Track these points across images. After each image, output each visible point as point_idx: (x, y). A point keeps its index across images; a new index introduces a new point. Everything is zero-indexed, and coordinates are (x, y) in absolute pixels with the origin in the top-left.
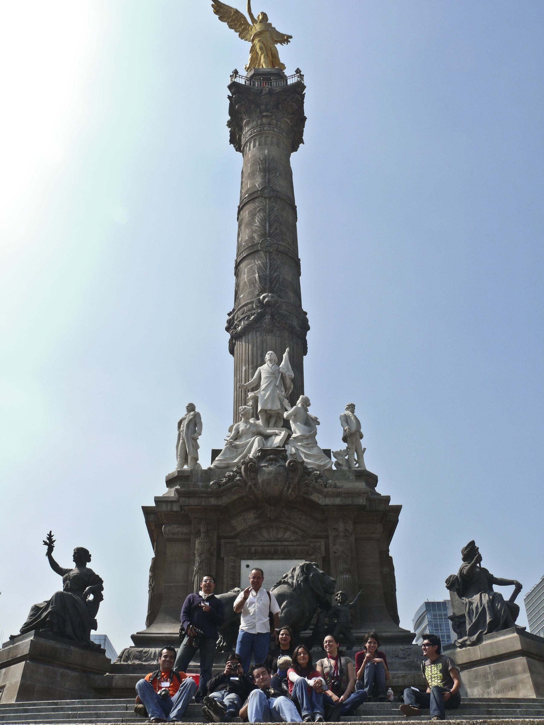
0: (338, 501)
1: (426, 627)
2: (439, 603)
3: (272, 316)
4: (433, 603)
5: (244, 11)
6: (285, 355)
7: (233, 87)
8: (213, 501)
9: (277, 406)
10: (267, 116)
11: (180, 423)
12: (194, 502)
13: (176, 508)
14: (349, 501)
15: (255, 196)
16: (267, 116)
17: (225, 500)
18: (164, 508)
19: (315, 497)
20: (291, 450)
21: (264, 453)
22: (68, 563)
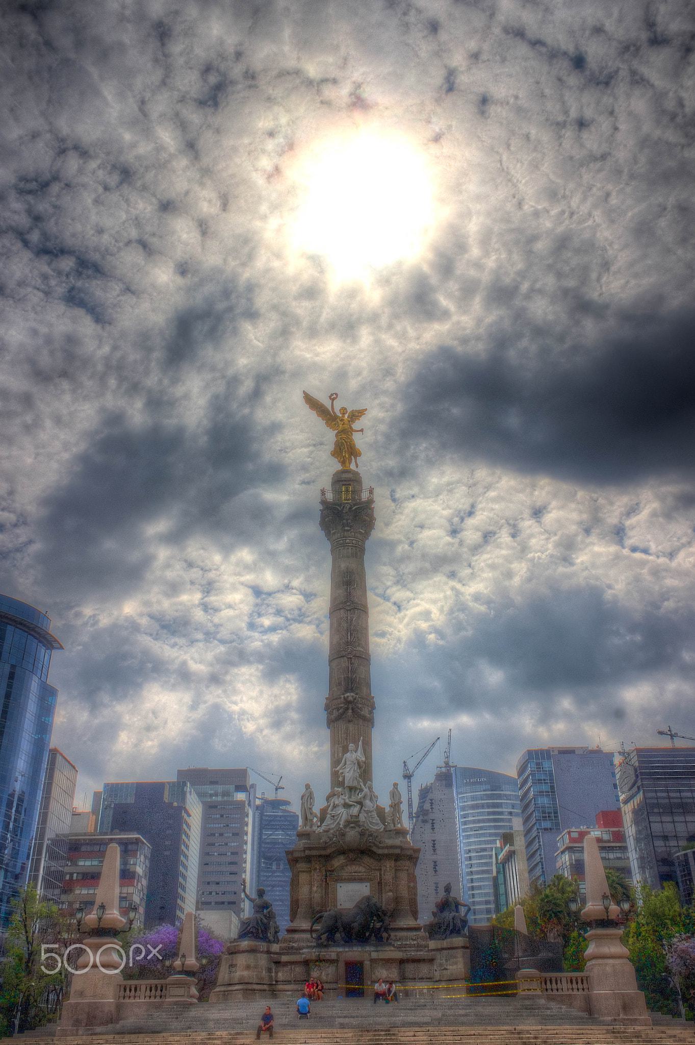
0: (386, 851)
1: (527, 778)
2: (542, 751)
3: (353, 709)
4: (536, 752)
5: (330, 408)
6: (360, 743)
7: (324, 502)
8: (323, 853)
9: (355, 784)
10: (348, 531)
11: (303, 797)
12: (314, 853)
13: (303, 855)
14: (391, 851)
15: (341, 606)
16: (348, 531)
17: (328, 851)
18: (296, 855)
19: (374, 849)
20: (362, 818)
21: (348, 823)
22: (254, 896)
